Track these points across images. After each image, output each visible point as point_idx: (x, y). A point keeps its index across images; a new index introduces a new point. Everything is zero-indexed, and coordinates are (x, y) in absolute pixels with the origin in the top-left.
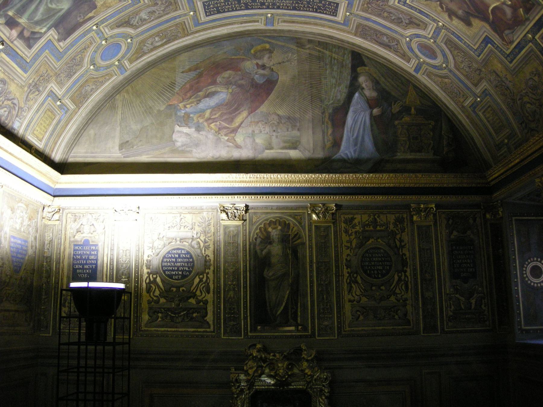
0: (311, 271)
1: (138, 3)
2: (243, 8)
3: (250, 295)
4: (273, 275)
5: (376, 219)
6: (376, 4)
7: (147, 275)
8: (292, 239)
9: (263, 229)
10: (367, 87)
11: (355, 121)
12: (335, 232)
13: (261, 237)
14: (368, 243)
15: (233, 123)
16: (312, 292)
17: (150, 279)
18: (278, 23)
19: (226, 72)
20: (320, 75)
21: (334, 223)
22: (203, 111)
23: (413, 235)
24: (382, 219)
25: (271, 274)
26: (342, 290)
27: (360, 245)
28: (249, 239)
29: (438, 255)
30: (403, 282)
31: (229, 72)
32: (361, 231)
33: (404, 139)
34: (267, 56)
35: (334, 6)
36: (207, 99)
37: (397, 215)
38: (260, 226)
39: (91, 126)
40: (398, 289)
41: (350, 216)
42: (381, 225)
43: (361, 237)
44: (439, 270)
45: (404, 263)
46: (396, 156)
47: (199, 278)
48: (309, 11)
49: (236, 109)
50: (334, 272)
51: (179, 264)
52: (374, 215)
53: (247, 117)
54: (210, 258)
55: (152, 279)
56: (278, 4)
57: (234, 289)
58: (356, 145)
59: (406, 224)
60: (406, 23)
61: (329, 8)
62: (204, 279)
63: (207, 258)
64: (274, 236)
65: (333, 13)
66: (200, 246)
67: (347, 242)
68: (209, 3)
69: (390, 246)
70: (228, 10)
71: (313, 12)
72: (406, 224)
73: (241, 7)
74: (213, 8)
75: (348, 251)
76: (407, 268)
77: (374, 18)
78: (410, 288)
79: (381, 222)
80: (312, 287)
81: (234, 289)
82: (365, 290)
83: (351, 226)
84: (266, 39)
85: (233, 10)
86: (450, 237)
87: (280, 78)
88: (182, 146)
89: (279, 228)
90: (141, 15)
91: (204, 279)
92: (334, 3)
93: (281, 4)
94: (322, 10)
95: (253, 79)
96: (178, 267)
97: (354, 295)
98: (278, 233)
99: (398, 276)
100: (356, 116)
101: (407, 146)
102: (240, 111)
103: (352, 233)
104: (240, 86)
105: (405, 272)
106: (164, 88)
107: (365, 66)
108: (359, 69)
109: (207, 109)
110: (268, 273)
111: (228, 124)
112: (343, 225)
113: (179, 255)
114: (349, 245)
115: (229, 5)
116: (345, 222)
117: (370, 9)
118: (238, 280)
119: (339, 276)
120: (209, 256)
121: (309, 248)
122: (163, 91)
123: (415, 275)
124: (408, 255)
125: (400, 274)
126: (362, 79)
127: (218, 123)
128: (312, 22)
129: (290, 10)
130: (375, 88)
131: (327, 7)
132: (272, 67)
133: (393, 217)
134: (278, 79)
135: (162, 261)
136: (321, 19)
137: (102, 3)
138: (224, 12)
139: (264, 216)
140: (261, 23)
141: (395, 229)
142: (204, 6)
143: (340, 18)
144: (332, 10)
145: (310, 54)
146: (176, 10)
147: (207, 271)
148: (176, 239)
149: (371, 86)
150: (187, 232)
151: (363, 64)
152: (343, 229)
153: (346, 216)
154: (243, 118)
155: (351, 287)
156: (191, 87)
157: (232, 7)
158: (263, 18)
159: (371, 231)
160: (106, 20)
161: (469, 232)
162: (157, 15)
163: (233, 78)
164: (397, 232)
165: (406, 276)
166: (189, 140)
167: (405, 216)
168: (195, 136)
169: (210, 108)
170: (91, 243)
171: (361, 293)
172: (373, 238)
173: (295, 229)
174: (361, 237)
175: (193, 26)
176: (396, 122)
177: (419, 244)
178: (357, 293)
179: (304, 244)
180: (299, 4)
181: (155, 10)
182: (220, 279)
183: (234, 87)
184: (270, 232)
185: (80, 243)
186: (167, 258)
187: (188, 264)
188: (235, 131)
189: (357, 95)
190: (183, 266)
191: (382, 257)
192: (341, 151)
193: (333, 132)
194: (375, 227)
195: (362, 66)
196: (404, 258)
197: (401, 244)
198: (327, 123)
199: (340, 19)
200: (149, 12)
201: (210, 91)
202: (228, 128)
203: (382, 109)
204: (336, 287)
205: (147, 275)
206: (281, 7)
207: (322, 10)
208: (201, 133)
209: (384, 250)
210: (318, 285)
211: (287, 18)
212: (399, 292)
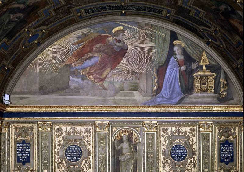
0: (144, 157)
3: (112, 170)
4: (124, 159)
5: (179, 129)
7: (57, 159)
8: (134, 140)
9: (118, 135)
10: (179, 53)
11: (170, 74)
12: (157, 137)
13: (118, 139)
14: (174, 142)
15: (102, 76)
16: (144, 168)
17: (59, 162)
19: (98, 44)
20: (152, 46)
21: (156, 132)
22: (86, 68)
23: (199, 138)
24: (183, 129)
25: (122, 159)
26: (160, 167)
27: (170, 143)
28: (111, 140)
29: (213, 149)
30: (192, 164)
31: (100, 44)
32: (171, 136)
33: (198, 84)
34: (121, 34)
36: (88, 61)
37: (191, 127)
38: (117, 133)
39: (22, 77)
40: (189, 167)
41: (166, 128)
42: (183, 133)
43: (171, 139)
44: (213, 157)
45: (194, 153)
46: (193, 94)
47: (85, 161)
49: (104, 67)
50: (156, 158)
51: (74, 153)
52: (178, 127)
53: (110, 72)
54: (91, 150)
55: (60, 161)
57: (103, 167)
58: (170, 88)
59: (196, 132)
62: (88, 161)
63: (89, 150)
64: (125, 139)
66: (85, 144)
67: (163, 142)
69: (186, 144)
72: (196, 132)
75: (164, 147)
76: (195, 156)
78: (196, 166)
79: (182, 131)
80: (144, 165)
81: (103, 167)
82: (172, 167)
83: (166, 133)
84: (121, 23)
86: (220, 139)
87: (128, 48)
88: (75, 88)
89: (127, 134)
91: (88, 161)
95: (113, 49)
96: (74, 155)
97: (166, 169)
98: (126, 137)
99: (190, 160)
100: (171, 71)
101: (199, 89)
102: (106, 68)
103: (166, 137)
104: (106, 53)
105: (194, 158)
106: (63, 54)
107: (178, 40)
108: (174, 42)
109: (87, 67)
110: (121, 158)
111: (100, 76)
112: (162, 133)
113: (74, 148)
114: (164, 143)
116: (163, 131)
118: (106, 162)
119: (158, 160)
120: (90, 149)
121: (143, 146)
122: (62, 56)
123: (199, 160)
124: (196, 149)
125: (191, 159)
126: (175, 48)
127: (94, 75)
130: (183, 54)
132: (124, 41)
133: (189, 128)
134: (128, 48)
135: (65, 152)
139: (119, 128)
141: (189, 135)
145: (146, 33)
147: (89, 157)
148: (72, 140)
149: (181, 53)
150: (78, 136)
151: (177, 39)
152: (161, 135)
153: (163, 128)
154: (108, 72)
155: (165, 165)
156: (78, 55)
159: (176, 136)
160: (32, 26)
161: (231, 137)
163: (102, 48)
164: (191, 137)
165: (194, 160)
166: (78, 85)
167: (195, 127)
168: (82, 83)
169: (89, 67)
170: (26, 142)
171: (169, 169)
172: (177, 139)
173: (135, 135)
174: (171, 139)
176: (194, 75)
177: (202, 143)
178: (168, 169)
179: (140, 143)
182: (96, 161)
183: (103, 54)
184: (122, 137)
185: (20, 142)
186: (68, 150)
187: (79, 154)
188: (103, 80)
189: (172, 58)
190: (76, 154)
191: (182, 150)
192: (162, 92)
193: (158, 81)
194: (179, 134)
195: (176, 40)
196: (194, 150)
197: (192, 143)
198: (155, 75)
201: (89, 56)
202: (99, 78)
203: (187, 66)
204: (157, 165)
205: (57, 159)
208: (85, 81)
209: (183, 146)
210: (148, 164)
212: (190, 169)
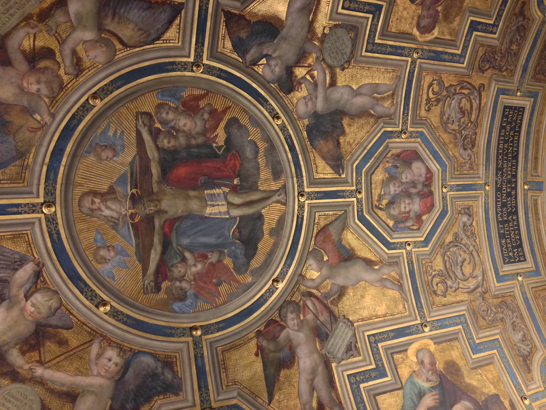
1: (499, 342)
2: (515, 218)
6: (501, 61)
18: (539, 176)
35: (509, 112)
48: (518, 140)
56: (509, 177)
60: (524, 20)
61: (512, 117)
65: (520, 111)
68: (506, 257)
70: (517, 234)
71: (519, 136)
73: (514, 220)
74: (514, 253)
77: (522, 61)
85: (519, 229)
90: (516, 341)
92: (504, 111)
93: (510, 173)
94: (516, 125)
115: (510, 233)
117: (509, 68)
128: (536, 135)
129: (517, 162)
131: (512, 119)
136: (530, 125)
137: (492, 387)
138: (520, 239)
140: (539, 196)
142: (509, 262)
143: (527, 103)
144: (516, 113)
146: (514, 297)
157: (512, 230)
158: (530, 194)
162: (518, 321)
175: (540, 277)
180: (508, 152)
181: (512, 321)
199: (528, 103)
200: (514, 330)
206: (514, 173)
207: (515, 126)
211: (529, 165)
